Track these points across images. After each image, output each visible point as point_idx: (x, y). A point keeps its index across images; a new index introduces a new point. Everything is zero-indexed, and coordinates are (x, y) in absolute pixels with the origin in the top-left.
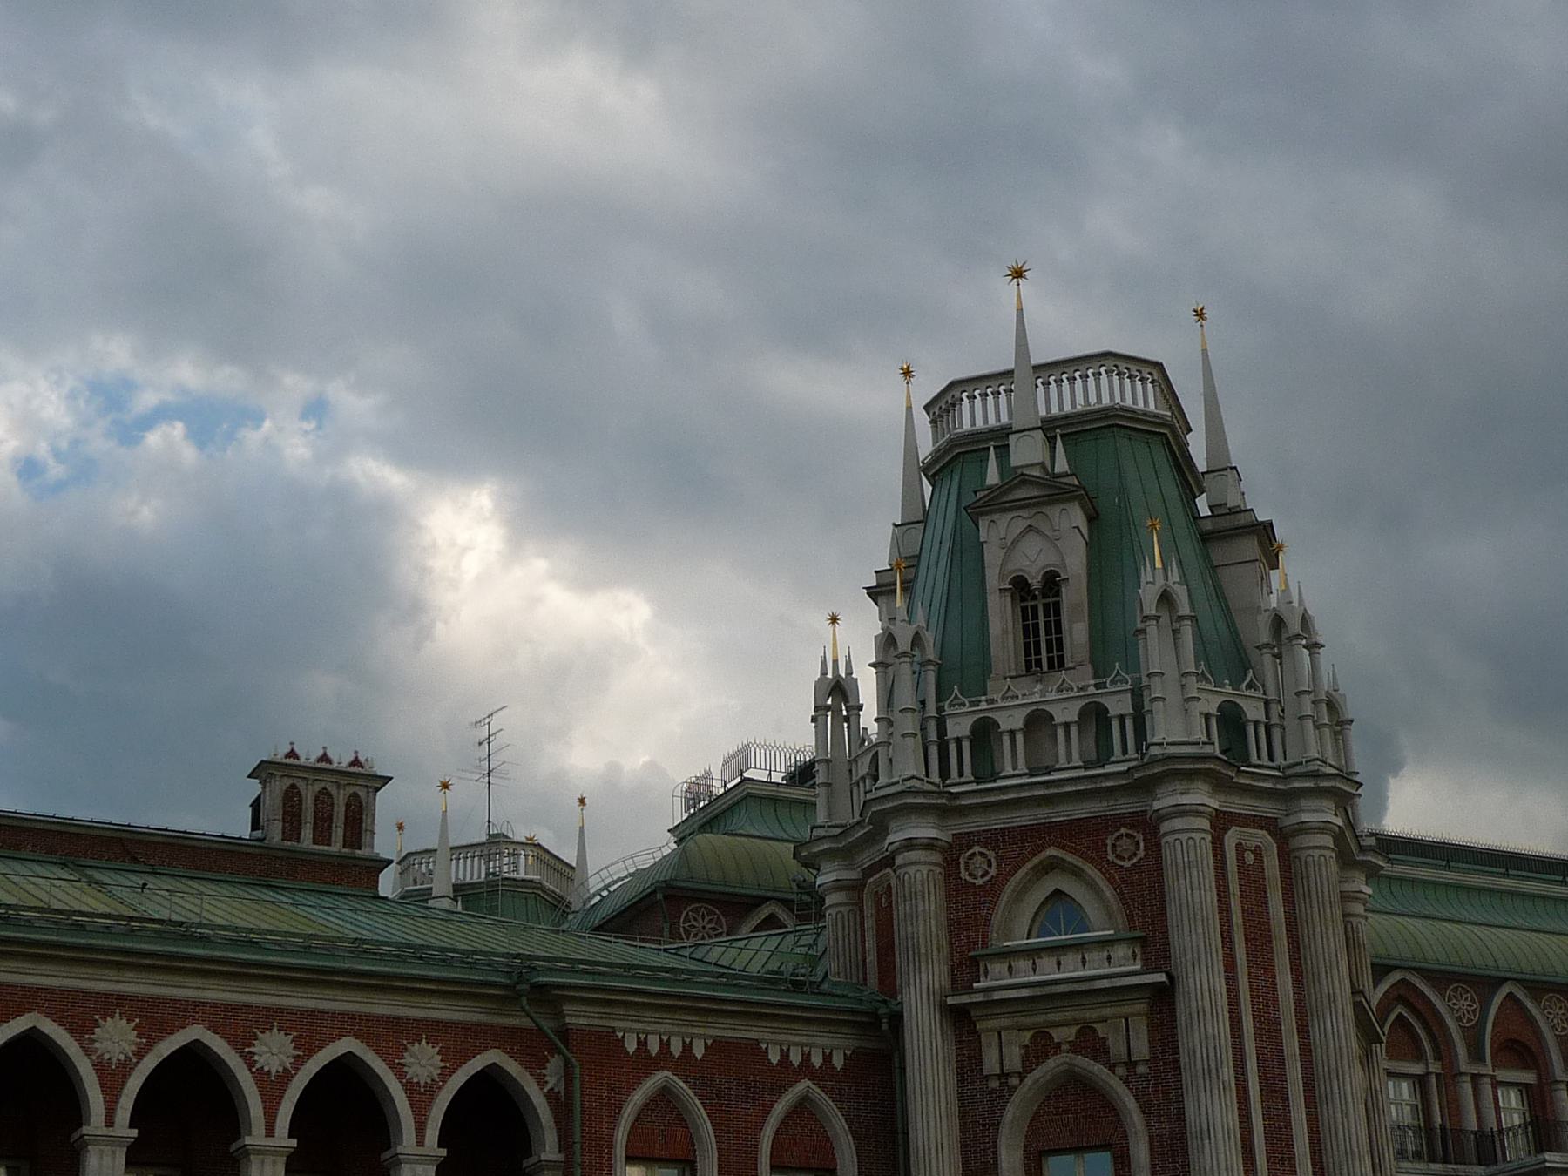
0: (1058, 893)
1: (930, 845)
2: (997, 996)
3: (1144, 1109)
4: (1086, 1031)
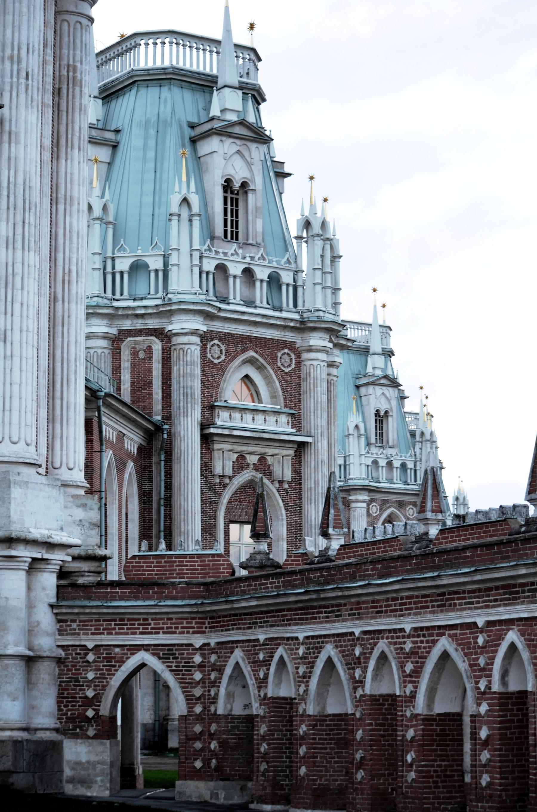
0: (247, 376)
1: (194, 333)
2: (235, 433)
3: (286, 506)
4: (263, 458)
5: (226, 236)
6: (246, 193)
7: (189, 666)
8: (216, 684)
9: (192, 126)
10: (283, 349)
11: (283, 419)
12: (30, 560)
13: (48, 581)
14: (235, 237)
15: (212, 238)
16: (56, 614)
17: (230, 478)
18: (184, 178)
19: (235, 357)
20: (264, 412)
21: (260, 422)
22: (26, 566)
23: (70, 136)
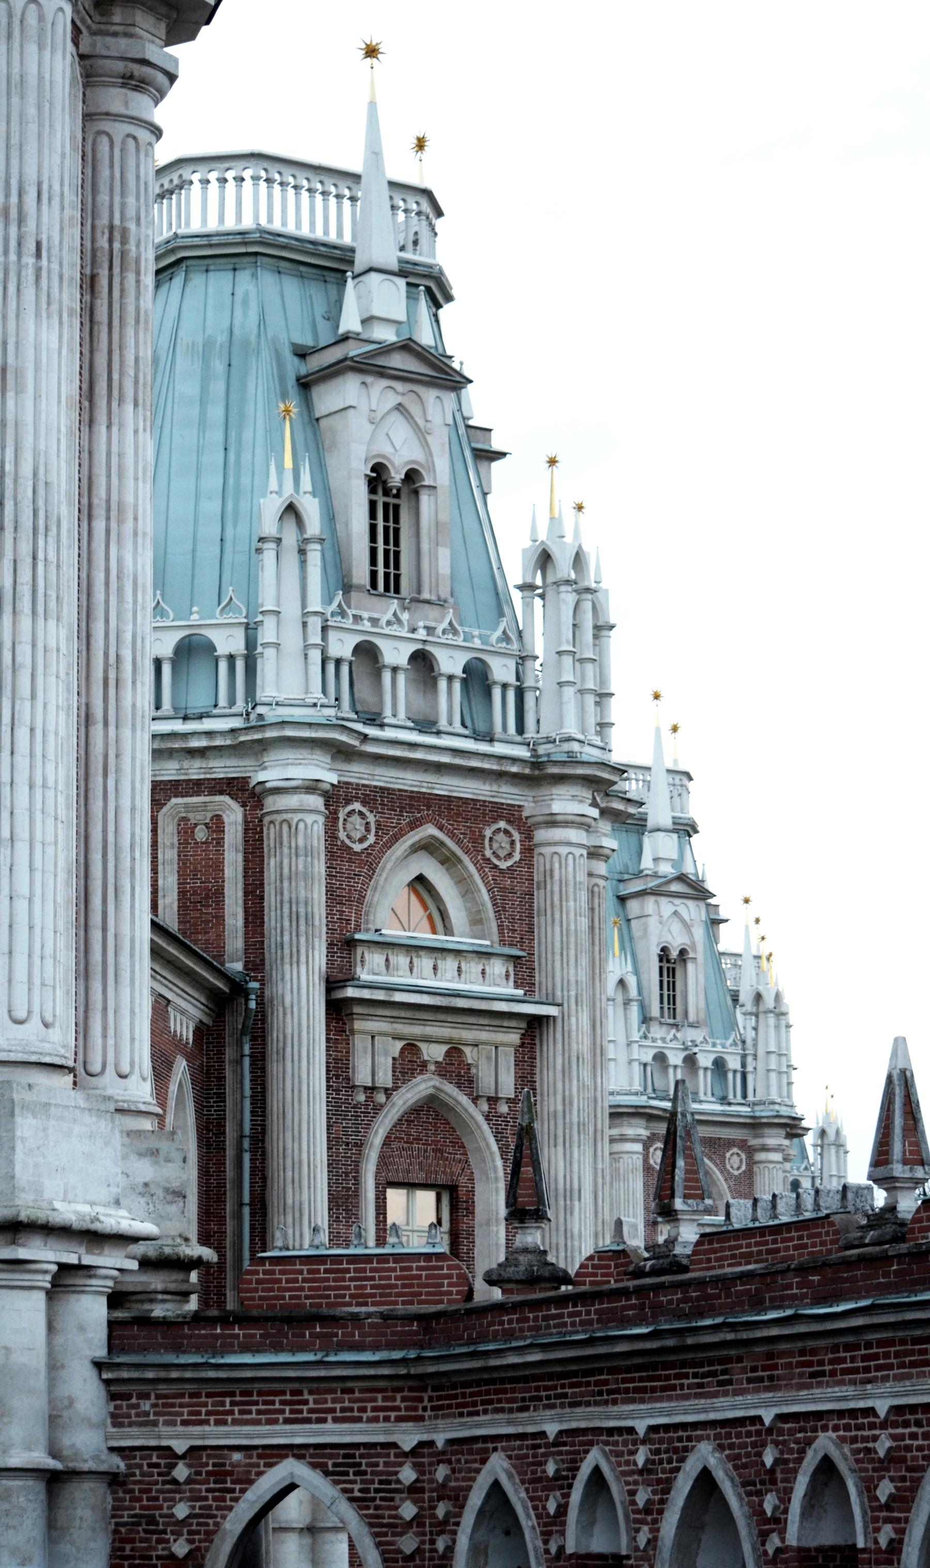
0: (421, 879)
1: (312, 787)
2: (399, 997)
4: (455, 1051)
5: (374, 585)
6: (416, 493)
7: (390, 1490)
8: (448, 1526)
9: (302, 354)
10: (495, 820)
11: (497, 968)
12: (54, 1268)
13: (91, 1312)
14: (393, 585)
15: (347, 588)
16: (107, 1382)
17: (388, 1092)
18: (288, 463)
19: (395, 838)
20: (457, 953)
21: (449, 975)
22: (45, 1281)
23: (116, 376)
